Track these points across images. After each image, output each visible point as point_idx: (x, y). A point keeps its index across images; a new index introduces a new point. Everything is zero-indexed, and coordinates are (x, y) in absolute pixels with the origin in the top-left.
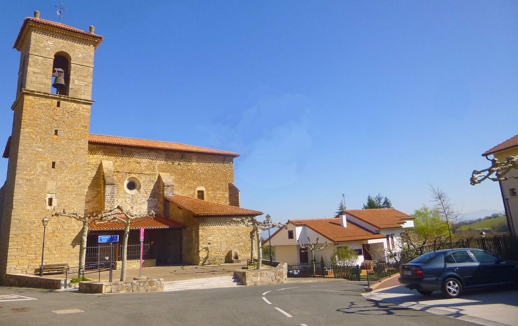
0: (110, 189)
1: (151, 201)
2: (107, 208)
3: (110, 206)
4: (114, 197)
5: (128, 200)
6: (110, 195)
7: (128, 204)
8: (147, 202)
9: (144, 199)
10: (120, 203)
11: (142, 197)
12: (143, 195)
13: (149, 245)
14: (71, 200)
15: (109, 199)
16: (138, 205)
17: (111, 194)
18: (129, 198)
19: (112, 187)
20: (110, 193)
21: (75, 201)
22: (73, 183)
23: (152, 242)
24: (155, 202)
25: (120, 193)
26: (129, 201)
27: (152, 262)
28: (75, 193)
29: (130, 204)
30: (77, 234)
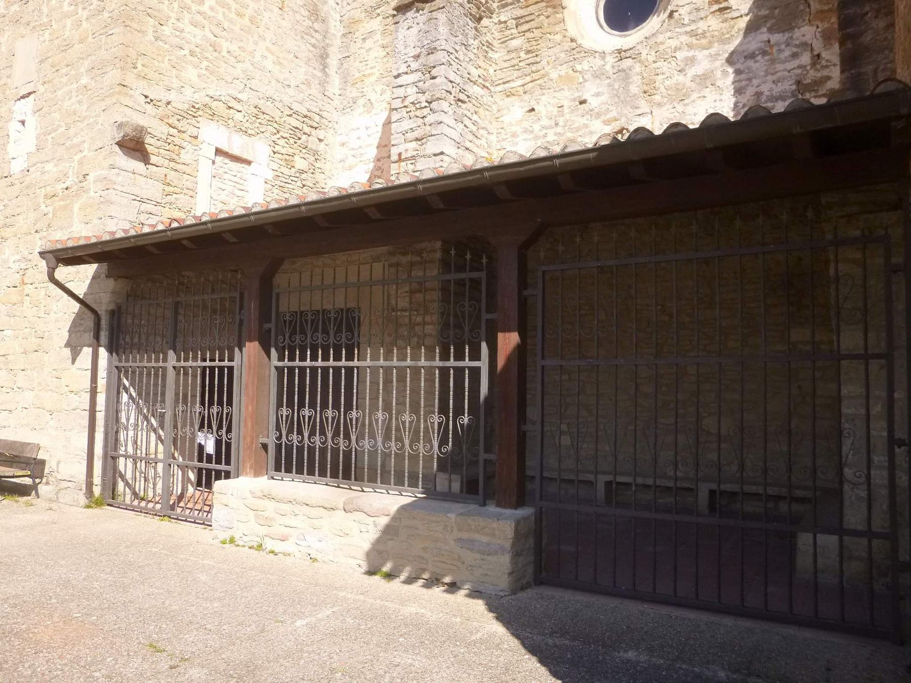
0: (415, 30)
1: (764, 53)
2: (401, 148)
3: (416, 134)
4: (434, 72)
5: (594, 90)
6: (414, 65)
7: (598, 115)
8: (725, 72)
9: (701, 55)
10: (545, 122)
11: (690, 46)
12: (693, 34)
13: (483, 364)
14: (73, 107)
15: (412, 90)
16: (659, 105)
17: (422, 60)
18: (598, 75)
19: (422, 17)
20: (417, 57)
21: (85, 107)
22: (85, 14)
23: (508, 341)
24: (795, 56)
25: (544, 63)
26: (598, 95)
27: (469, 544)
28: (87, 63)
29: (608, 111)
30: (88, 282)
